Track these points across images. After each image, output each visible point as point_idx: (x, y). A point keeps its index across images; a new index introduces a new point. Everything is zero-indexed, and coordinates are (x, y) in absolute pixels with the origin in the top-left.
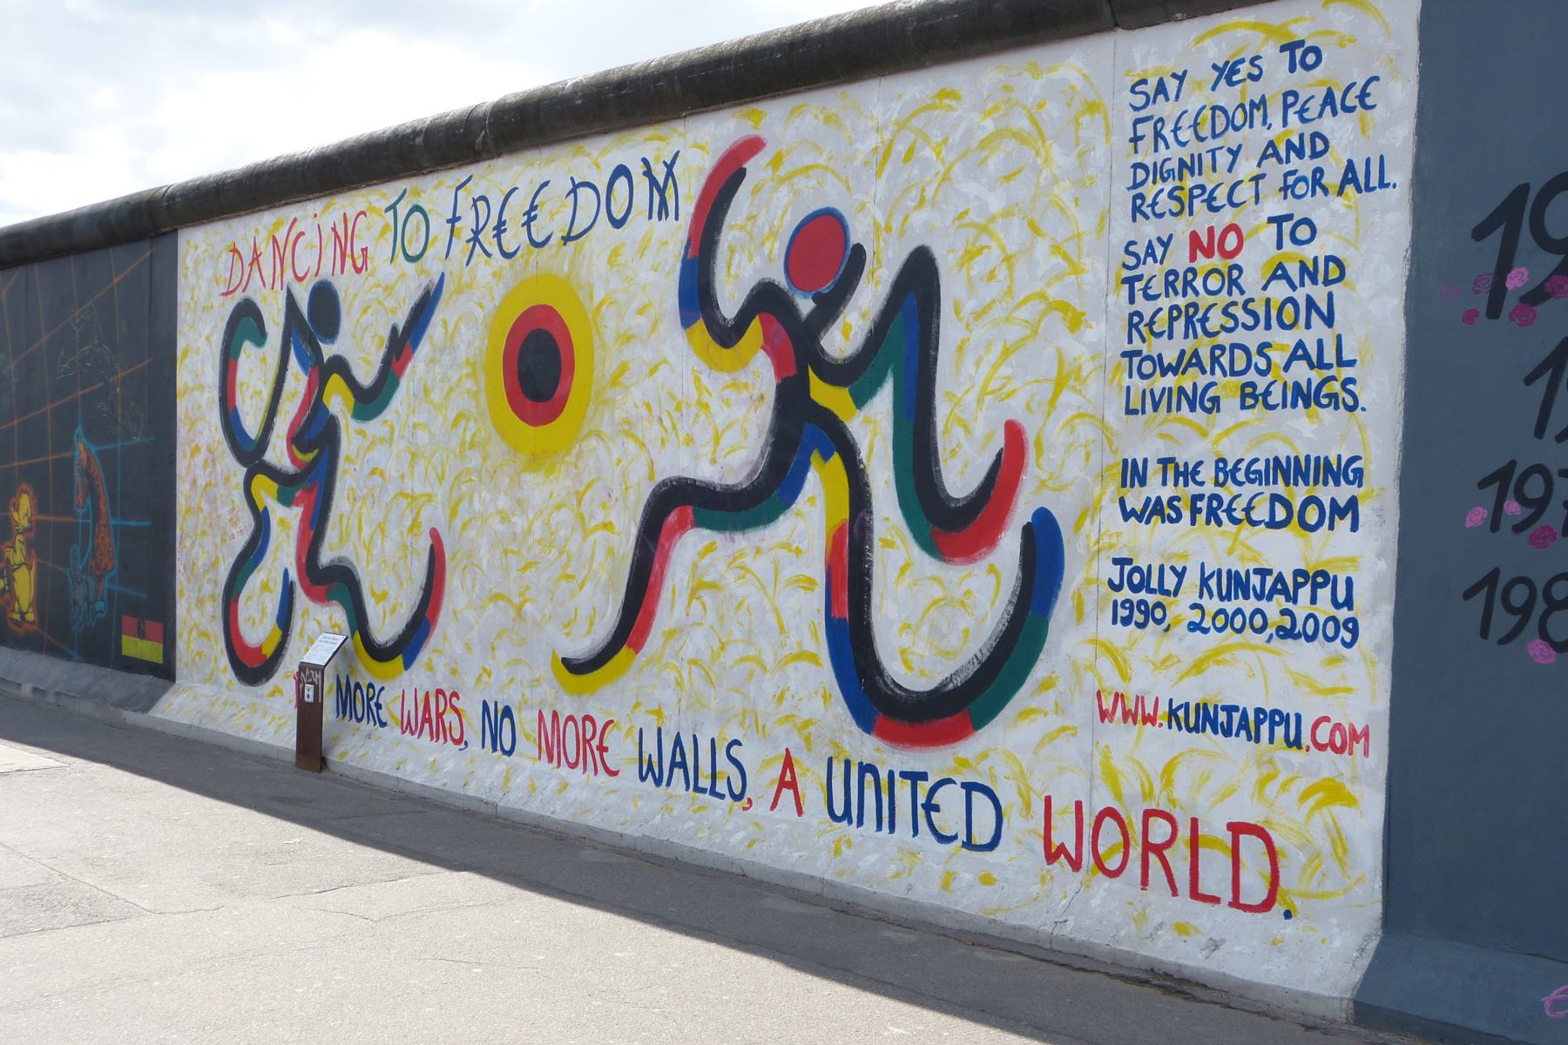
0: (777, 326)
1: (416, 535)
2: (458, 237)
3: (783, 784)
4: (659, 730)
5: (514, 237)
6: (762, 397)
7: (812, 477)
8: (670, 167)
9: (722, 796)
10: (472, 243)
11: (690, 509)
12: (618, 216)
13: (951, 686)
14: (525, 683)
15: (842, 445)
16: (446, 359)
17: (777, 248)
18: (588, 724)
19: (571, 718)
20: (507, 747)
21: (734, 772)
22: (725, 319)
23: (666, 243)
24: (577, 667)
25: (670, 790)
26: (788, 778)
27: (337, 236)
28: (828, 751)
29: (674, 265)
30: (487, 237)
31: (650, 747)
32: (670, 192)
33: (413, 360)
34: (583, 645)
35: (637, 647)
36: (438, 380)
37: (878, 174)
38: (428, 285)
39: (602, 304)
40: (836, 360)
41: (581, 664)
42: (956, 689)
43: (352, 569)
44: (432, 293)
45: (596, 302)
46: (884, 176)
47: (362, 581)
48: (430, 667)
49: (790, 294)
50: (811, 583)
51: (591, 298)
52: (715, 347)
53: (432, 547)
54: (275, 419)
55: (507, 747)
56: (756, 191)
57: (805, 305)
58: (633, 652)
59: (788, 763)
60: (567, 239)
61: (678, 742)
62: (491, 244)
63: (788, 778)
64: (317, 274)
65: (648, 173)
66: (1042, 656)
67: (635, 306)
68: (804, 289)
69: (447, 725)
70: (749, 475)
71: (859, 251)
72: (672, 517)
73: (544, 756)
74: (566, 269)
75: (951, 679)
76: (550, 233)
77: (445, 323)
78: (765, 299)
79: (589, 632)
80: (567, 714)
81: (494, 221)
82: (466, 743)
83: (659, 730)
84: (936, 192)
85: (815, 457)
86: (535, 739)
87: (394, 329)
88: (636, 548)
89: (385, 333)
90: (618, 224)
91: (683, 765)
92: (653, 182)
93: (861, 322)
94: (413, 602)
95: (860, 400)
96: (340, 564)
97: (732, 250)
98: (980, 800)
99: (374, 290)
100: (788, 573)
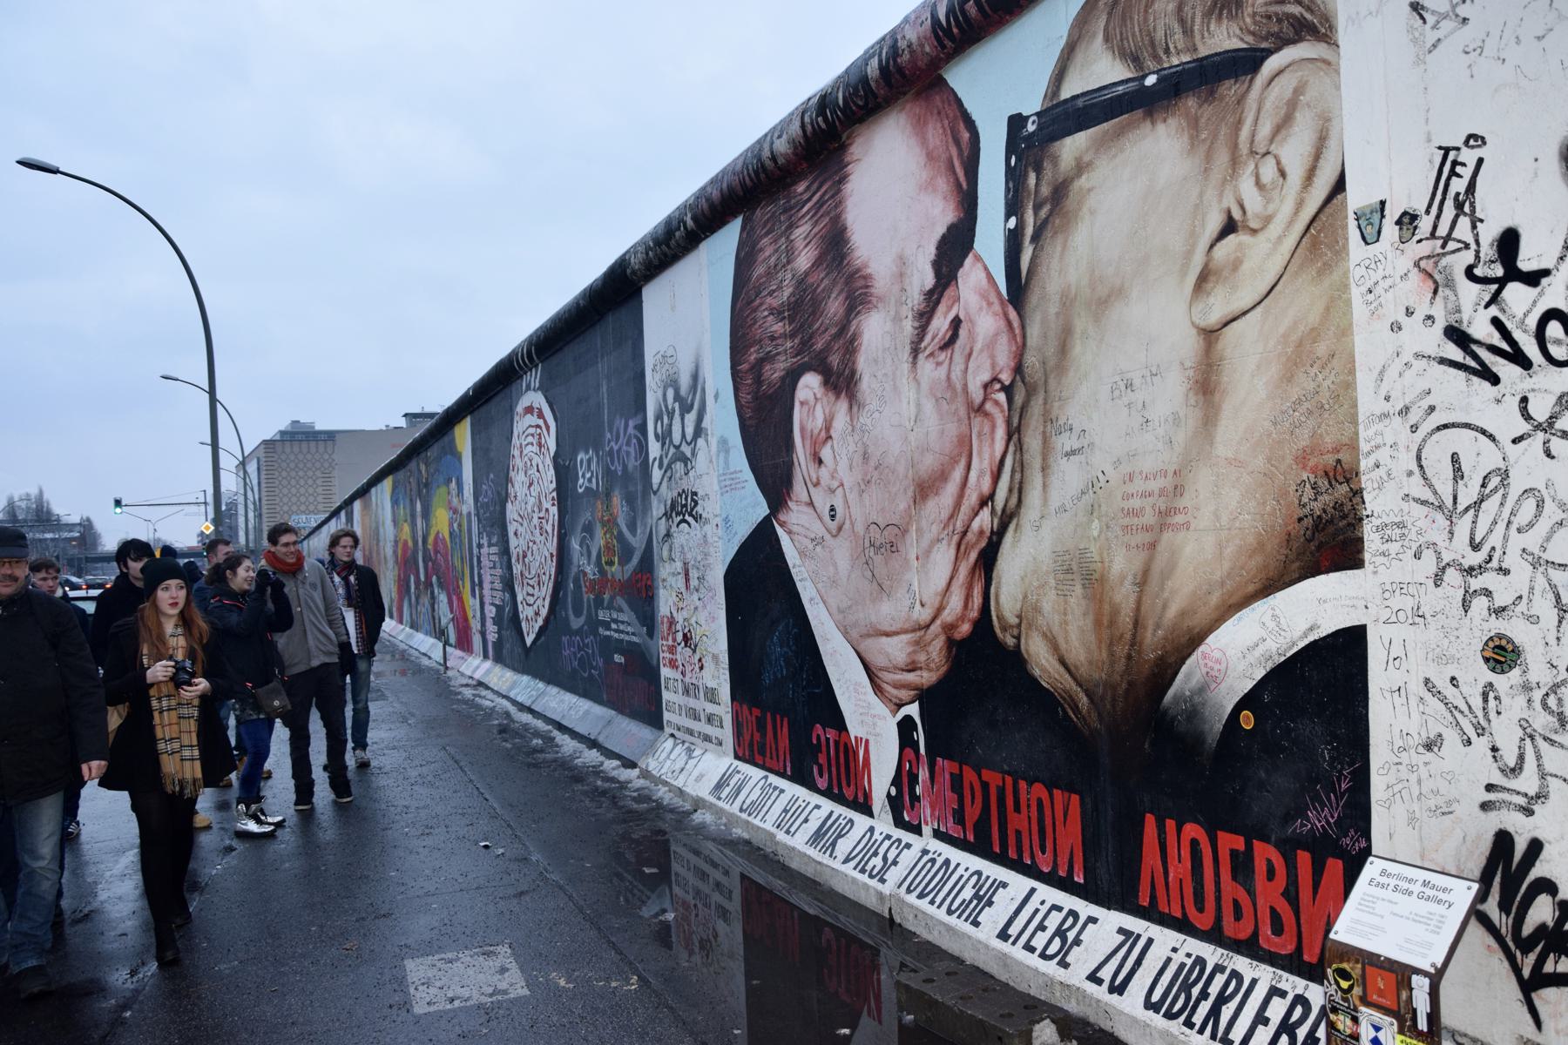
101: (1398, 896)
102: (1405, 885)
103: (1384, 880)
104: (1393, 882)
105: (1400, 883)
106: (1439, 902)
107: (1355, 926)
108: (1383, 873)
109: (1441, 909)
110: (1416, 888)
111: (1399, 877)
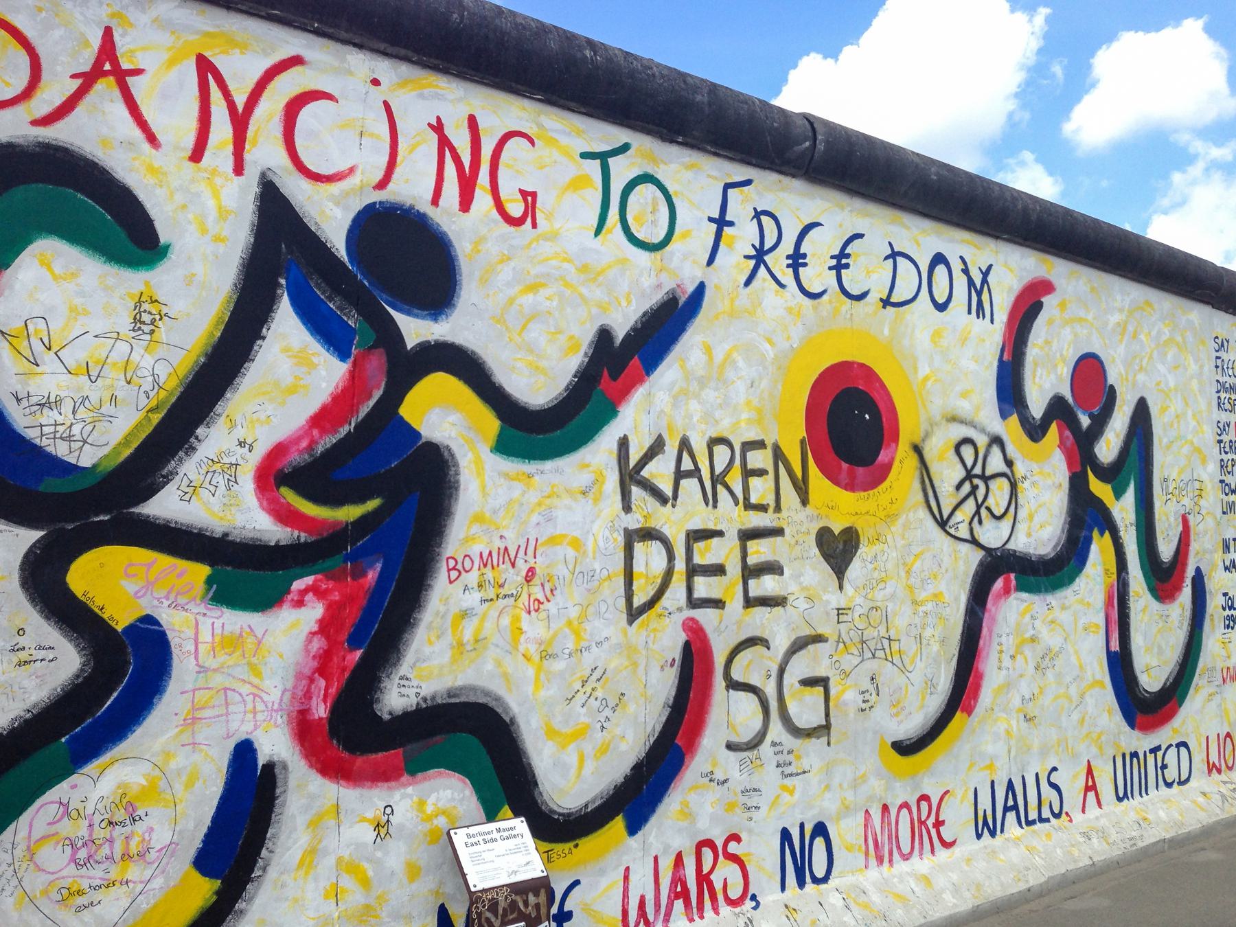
0: (1068, 433)
1: (655, 630)
2: (730, 247)
3: (1088, 789)
4: (993, 782)
5: (817, 275)
6: (1060, 485)
7: (1094, 548)
8: (986, 274)
9: (1047, 820)
10: (752, 263)
11: (1012, 576)
12: (941, 300)
13: (1168, 684)
14: (845, 786)
15: (1108, 524)
16: (710, 395)
17: (1065, 371)
18: (924, 805)
19: (905, 805)
20: (820, 873)
21: (1054, 793)
22: (1034, 418)
23: (984, 341)
24: (906, 748)
25: (1006, 835)
26: (1090, 783)
27: (444, 143)
28: (1111, 752)
29: (991, 363)
30: (778, 261)
31: (985, 803)
32: (985, 297)
33: (646, 385)
34: (911, 725)
35: (969, 711)
36: (695, 420)
37: (1121, 341)
38: (673, 289)
39: (926, 379)
40: (1103, 464)
41: (914, 742)
42: (1171, 684)
43: (492, 704)
44: (681, 302)
45: (921, 375)
46: (1124, 343)
47: (521, 721)
48: (688, 814)
49: (1075, 409)
50: (1097, 626)
51: (916, 369)
52: (1025, 439)
53: (687, 646)
54: (200, 431)
55: (820, 873)
56: (1051, 322)
57: (1085, 421)
58: (965, 715)
59: (1090, 772)
60: (886, 302)
61: (1010, 786)
62: (784, 274)
63: (1090, 783)
64: (382, 185)
65: (966, 271)
66: (1201, 654)
67: (958, 389)
68: (1085, 409)
69: (718, 886)
70: (1055, 547)
71: (1112, 387)
72: (999, 584)
73: (873, 861)
74: (886, 332)
75: (1167, 679)
76: (866, 289)
77: (708, 350)
78: (1058, 409)
79: (922, 707)
80: (899, 802)
81: (787, 247)
82: (754, 898)
83: (993, 782)
84: (1147, 364)
85: (1096, 534)
86: (860, 847)
87: (604, 335)
88: (966, 615)
89: (586, 337)
90: (941, 307)
91: (1015, 807)
92: (971, 282)
93: (1116, 440)
94: (649, 729)
95: (1118, 494)
96: (453, 700)
97: (1036, 364)
98: (1183, 750)
99: (554, 262)
100: (1083, 621)
101: (490, 845)
102: (489, 837)
103: (473, 840)
104: (480, 838)
105: (483, 837)
106: (515, 836)
107: (482, 875)
108: (468, 836)
109: (518, 840)
110: (496, 835)
111: (480, 834)
